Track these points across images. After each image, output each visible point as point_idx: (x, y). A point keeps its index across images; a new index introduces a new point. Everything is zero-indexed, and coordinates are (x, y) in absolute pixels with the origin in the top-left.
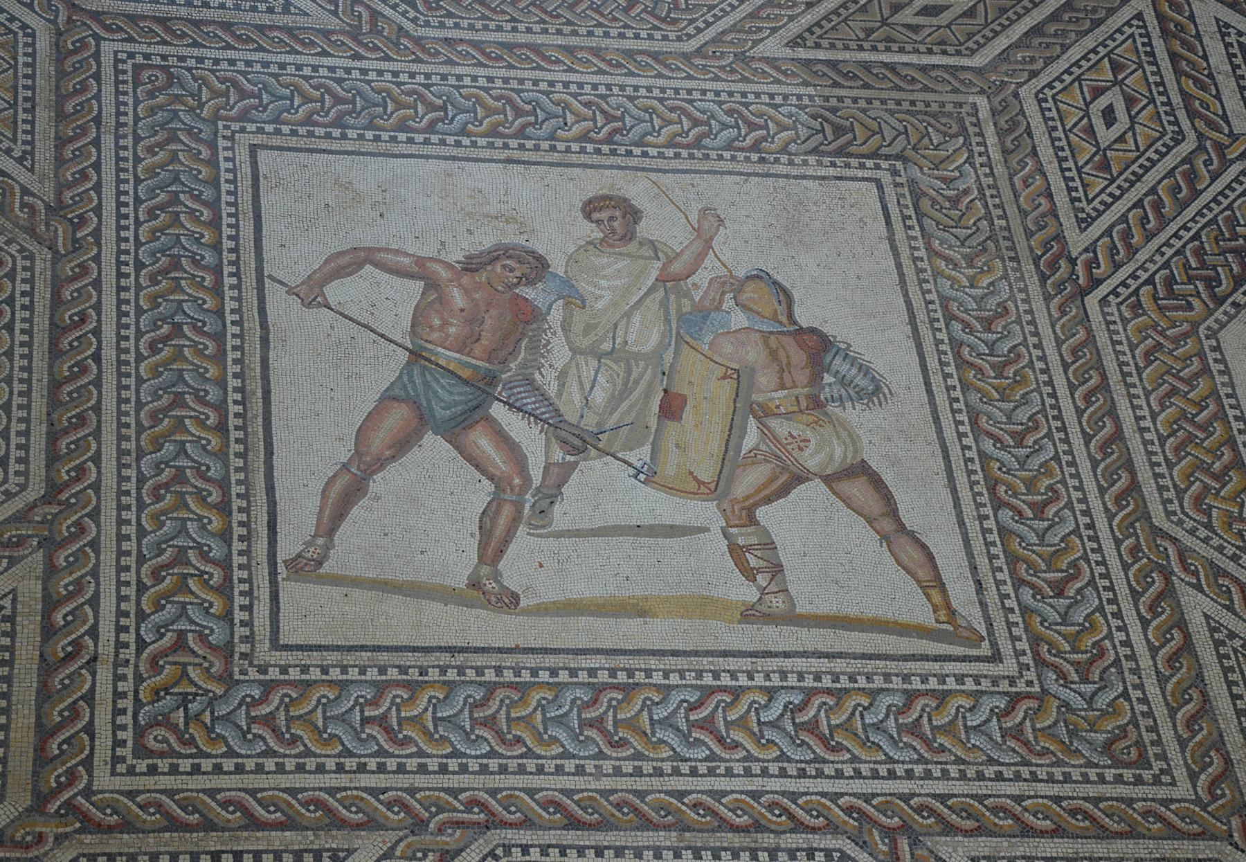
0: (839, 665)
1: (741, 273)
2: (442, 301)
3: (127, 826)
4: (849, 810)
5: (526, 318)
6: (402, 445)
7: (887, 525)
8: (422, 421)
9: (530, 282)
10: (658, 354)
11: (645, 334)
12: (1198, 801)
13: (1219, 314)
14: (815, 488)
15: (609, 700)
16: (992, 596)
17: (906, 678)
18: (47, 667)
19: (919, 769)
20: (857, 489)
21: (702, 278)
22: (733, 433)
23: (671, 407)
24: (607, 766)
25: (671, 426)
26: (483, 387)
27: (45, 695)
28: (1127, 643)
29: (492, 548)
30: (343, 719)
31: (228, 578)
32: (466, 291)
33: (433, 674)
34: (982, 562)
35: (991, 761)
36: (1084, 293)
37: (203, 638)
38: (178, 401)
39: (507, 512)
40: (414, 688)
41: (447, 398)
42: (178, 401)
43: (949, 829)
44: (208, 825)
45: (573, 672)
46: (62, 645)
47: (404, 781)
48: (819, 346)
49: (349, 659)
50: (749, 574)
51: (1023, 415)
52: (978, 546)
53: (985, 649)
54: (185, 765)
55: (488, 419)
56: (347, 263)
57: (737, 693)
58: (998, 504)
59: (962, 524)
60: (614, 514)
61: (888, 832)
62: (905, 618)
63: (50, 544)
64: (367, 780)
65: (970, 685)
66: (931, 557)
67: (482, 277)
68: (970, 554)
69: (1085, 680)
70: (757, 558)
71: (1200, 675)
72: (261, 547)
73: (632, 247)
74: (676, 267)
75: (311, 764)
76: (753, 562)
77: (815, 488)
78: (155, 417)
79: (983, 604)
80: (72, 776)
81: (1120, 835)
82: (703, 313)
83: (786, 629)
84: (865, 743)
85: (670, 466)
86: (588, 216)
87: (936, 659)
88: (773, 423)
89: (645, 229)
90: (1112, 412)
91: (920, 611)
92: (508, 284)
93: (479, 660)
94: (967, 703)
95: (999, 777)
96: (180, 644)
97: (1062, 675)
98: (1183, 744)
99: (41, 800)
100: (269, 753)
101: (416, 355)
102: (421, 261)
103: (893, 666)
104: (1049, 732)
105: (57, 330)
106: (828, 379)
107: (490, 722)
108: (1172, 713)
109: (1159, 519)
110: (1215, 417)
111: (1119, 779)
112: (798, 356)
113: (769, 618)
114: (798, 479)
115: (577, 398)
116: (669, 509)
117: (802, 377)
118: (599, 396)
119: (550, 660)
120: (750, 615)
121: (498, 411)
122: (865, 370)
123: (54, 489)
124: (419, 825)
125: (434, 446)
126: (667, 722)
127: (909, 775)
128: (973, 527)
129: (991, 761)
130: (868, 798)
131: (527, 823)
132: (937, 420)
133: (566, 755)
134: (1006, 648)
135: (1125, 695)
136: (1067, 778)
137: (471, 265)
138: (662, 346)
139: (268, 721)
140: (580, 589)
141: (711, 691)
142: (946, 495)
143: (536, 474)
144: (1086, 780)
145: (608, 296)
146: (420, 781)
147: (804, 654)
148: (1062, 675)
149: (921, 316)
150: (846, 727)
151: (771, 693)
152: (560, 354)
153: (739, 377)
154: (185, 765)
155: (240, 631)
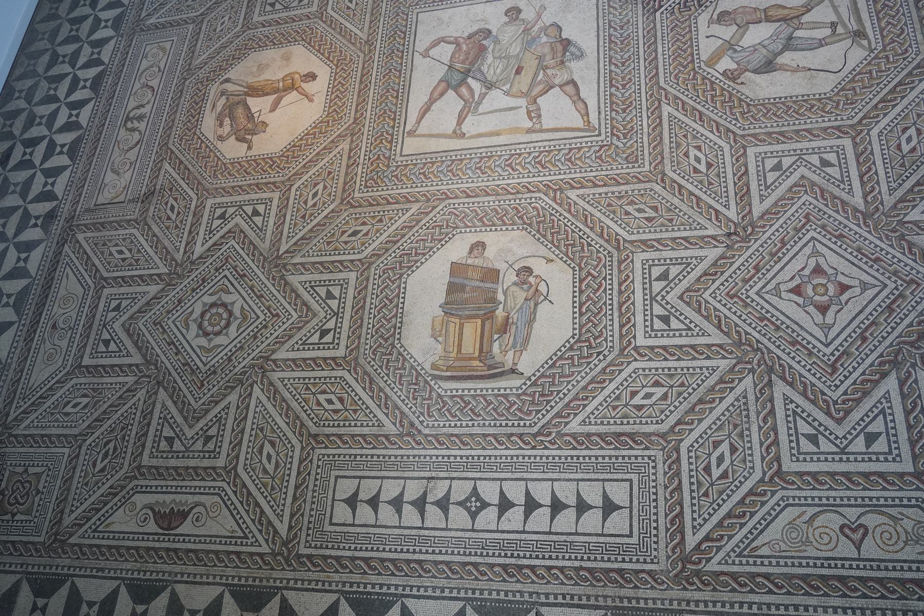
0: (552, 143)
1: (548, 24)
2: (460, 49)
3: (360, 206)
4: (544, 186)
5: (482, 49)
6: (442, 94)
7: (575, 98)
8: (449, 86)
9: (485, 39)
10: (518, 55)
11: (515, 49)
12: (650, 172)
13: (700, 11)
14: (557, 90)
15: (484, 161)
16: (603, 115)
17: (571, 144)
18: (348, 167)
19: (568, 171)
20: (570, 89)
21: (536, 28)
22: (536, 75)
23: (518, 72)
24: (480, 180)
25: (518, 76)
26: (467, 73)
27: (347, 174)
28: (641, 125)
29: (461, 120)
30: (414, 174)
31: (392, 139)
32: (467, 45)
33: (439, 159)
34: (602, 106)
35: (590, 166)
36: (656, 11)
37: (384, 155)
38: (388, 91)
39: (467, 109)
40: (433, 163)
41: (457, 77)
42: (388, 91)
43: (573, 187)
44: (378, 204)
45: (476, 154)
46: (352, 161)
47: (427, 189)
48: (567, 43)
49: (418, 157)
50: (531, 119)
51: (626, 56)
52: (602, 101)
53: (597, 132)
54: (375, 189)
55: (467, 83)
56: (435, 44)
57: (520, 155)
58: (612, 86)
59: (599, 94)
60: (496, 106)
61: (555, 191)
62: (574, 126)
63: (352, 135)
64: (417, 190)
65: (589, 144)
66: (586, 106)
67: (472, 40)
68: (599, 103)
69: (625, 138)
70: (534, 114)
71: (661, 133)
72: (402, 129)
73: (517, 22)
74: (529, 26)
75: (424, 185)
76: (533, 115)
77: (558, 88)
78: (381, 97)
79: (599, 119)
80: (350, 194)
81: (623, 184)
82: (534, 39)
83: (538, 134)
84: (555, 165)
85: (514, 90)
86: (506, 14)
87: (574, 138)
88: (548, 71)
89: (522, 16)
90: (656, 51)
91: (580, 123)
92: (479, 41)
93: (451, 153)
94: (586, 150)
95: (591, 171)
96: (378, 158)
97: (618, 138)
98: (650, 154)
99: (343, 200)
100: (395, 184)
101: (450, 67)
102: (456, 38)
103: (567, 141)
104: (610, 156)
105: (362, 76)
106: (568, 54)
107: (451, 171)
108: (650, 144)
109: (662, 84)
110: (689, 47)
111: (628, 167)
112: (560, 48)
113: (534, 132)
114: (552, 87)
115: (492, 72)
116: (511, 102)
117: (559, 55)
118: (498, 71)
119: (471, 151)
120: (529, 131)
121: (470, 80)
122: (580, 49)
123: (355, 119)
124: (428, 200)
125: (451, 93)
126: (499, 166)
127: (565, 173)
128: (602, 94)
129: (590, 166)
130: (551, 181)
131: (456, 197)
132: (598, 61)
133: (470, 178)
134: (603, 131)
135: (636, 141)
136: (612, 169)
137: (470, 37)
138: (520, 52)
139: (396, 176)
140: (482, 130)
141: (512, 155)
142: (596, 86)
143: (476, 97)
144: (617, 168)
145: (507, 39)
146: (431, 188)
147: (542, 141)
148: (618, 138)
149: (601, 28)
150: (549, 161)
151: (530, 153)
152: (490, 59)
153: (540, 58)
154: (375, 189)
155: (393, 153)
